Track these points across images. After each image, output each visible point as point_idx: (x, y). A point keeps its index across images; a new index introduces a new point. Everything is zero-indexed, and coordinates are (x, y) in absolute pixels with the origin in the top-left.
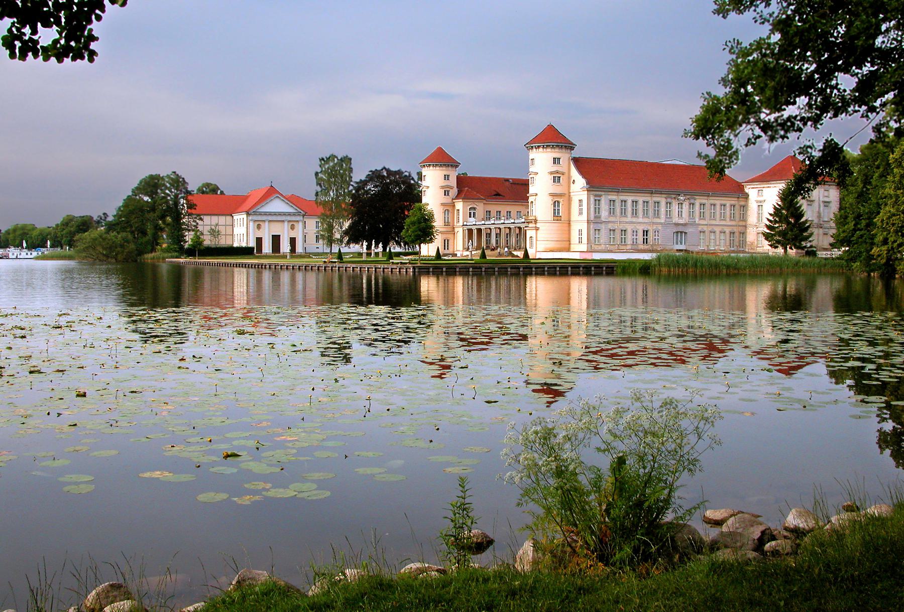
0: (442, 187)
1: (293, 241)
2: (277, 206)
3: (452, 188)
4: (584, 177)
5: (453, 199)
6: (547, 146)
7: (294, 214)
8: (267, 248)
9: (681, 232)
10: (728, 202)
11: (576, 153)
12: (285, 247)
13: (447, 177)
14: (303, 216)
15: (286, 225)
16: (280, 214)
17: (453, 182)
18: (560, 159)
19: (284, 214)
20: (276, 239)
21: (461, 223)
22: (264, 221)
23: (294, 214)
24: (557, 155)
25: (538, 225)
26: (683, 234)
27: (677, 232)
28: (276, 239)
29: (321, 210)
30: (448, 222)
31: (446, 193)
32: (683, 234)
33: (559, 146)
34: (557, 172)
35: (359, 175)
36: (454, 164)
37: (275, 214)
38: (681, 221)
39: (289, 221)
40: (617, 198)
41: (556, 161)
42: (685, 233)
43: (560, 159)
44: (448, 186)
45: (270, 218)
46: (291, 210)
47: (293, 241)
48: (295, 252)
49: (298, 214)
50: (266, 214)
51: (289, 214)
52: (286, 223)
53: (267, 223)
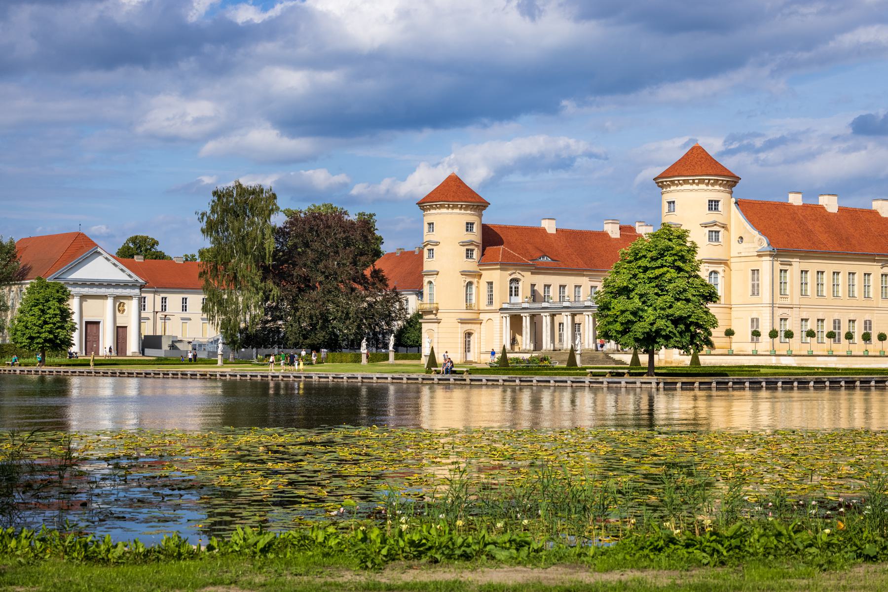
0: (463, 244)
4: (762, 232)
6: (683, 180)
7: (125, 285)
13: (469, 226)
16: (100, 284)
17: (476, 235)
18: (718, 201)
19: (109, 284)
21: (496, 305)
23: (125, 285)
24: (714, 196)
25: (439, 316)
30: (471, 305)
31: (469, 254)
33: (718, 180)
34: (715, 224)
36: (479, 205)
37: (92, 284)
41: (713, 205)
43: (718, 201)
44: (471, 243)
45: (86, 291)
47: (120, 332)
51: (117, 285)
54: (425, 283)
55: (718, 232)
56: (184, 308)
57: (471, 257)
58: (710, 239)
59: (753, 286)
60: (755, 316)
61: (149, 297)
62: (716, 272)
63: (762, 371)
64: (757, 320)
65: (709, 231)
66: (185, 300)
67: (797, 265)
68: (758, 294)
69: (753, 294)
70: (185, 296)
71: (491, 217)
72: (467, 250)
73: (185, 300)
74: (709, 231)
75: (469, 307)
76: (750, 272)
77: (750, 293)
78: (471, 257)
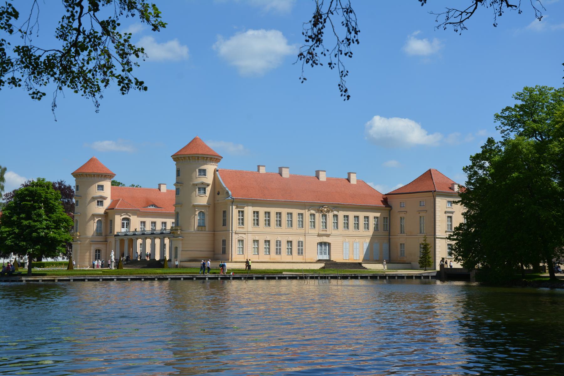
3: (105, 198)
9: (325, 244)
60: (224, 239)
64: (225, 240)
68: (226, 225)
72: (97, 201)
77: (222, 224)
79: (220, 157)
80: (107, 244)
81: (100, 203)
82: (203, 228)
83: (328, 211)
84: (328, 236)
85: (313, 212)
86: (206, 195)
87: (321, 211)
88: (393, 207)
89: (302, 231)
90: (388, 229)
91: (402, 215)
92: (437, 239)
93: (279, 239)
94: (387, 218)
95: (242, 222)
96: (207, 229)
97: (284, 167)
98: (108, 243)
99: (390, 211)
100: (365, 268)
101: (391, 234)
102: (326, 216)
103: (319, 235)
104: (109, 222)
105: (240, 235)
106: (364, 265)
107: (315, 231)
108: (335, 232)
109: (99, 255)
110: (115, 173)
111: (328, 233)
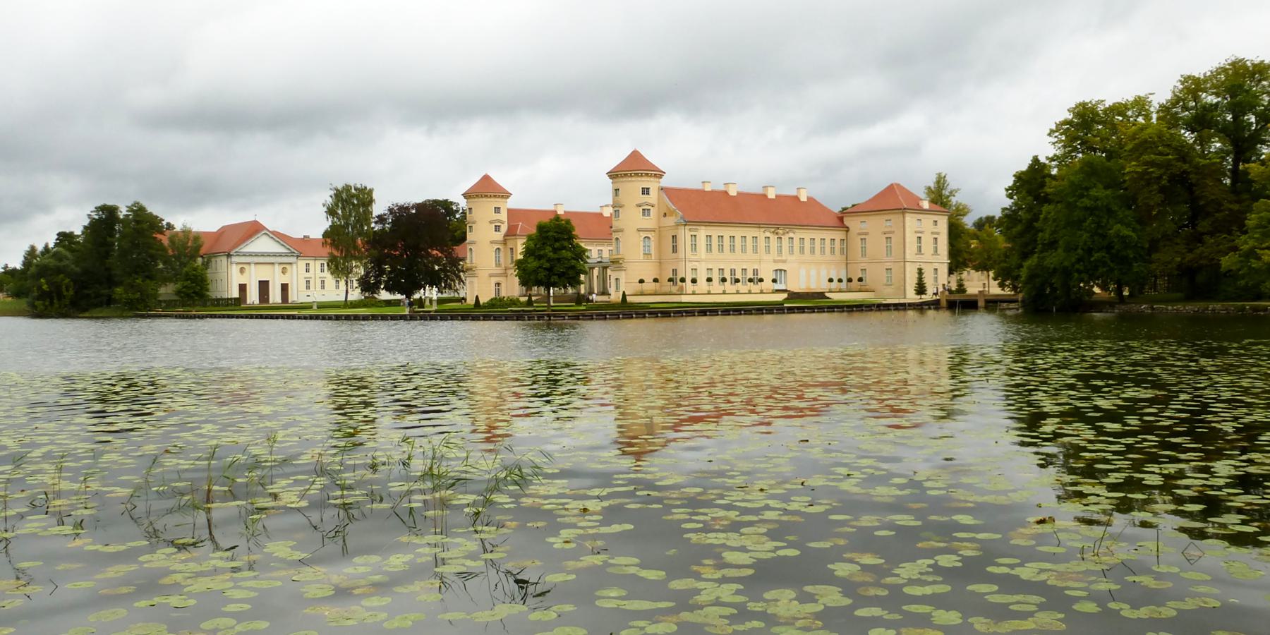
1: (285, 288)
2: (262, 244)
5: (505, 236)
8: (253, 297)
9: (781, 270)
10: (828, 235)
11: (664, 182)
12: (275, 296)
13: (497, 210)
14: (298, 256)
15: (278, 269)
16: (269, 255)
17: (503, 216)
19: (275, 255)
20: (264, 286)
22: (249, 263)
26: (783, 272)
27: (776, 270)
28: (264, 286)
29: (328, 250)
31: (497, 228)
32: (783, 272)
35: (379, 209)
37: (263, 255)
38: (780, 258)
39: (281, 263)
40: (715, 232)
42: (785, 271)
46: (282, 250)
47: (285, 288)
48: (267, 301)
49: (291, 254)
50: (250, 255)
51: (280, 255)
52: (277, 266)
53: (253, 266)
54: (468, 250)
55: (649, 209)
56: (307, 271)
57: (499, 231)
58: (644, 214)
59: (673, 246)
61: (311, 263)
62: (648, 238)
63: (652, 306)
65: (643, 209)
66: (308, 265)
67: (702, 232)
69: (673, 252)
70: (308, 262)
71: (512, 203)
72: (496, 226)
73: (308, 265)
74: (643, 209)
75: (498, 265)
76: (671, 238)
78: (499, 231)
79: (662, 172)
80: (507, 276)
81: (497, 228)
82: (649, 256)
83: (784, 234)
84: (784, 261)
85: (768, 234)
86: (652, 217)
87: (777, 233)
88: (851, 228)
89: (755, 256)
90: (845, 253)
91: (863, 237)
92: (907, 263)
93: (733, 267)
94: (844, 240)
95: (694, 247)
96: (653, 258)
97: (770, 186)
98: (509, 275)
99: (847, 231)
100: (828, 298)
101: (848, 259)
102: (781, 238)
103: (775, 261)
104: (509, 251)
105: (694, 263)
106: (827, 295)
107: (771, 257)
108: (790, 258)
109: (498, 289)
110: (510, 192)
111: (784, 258)
